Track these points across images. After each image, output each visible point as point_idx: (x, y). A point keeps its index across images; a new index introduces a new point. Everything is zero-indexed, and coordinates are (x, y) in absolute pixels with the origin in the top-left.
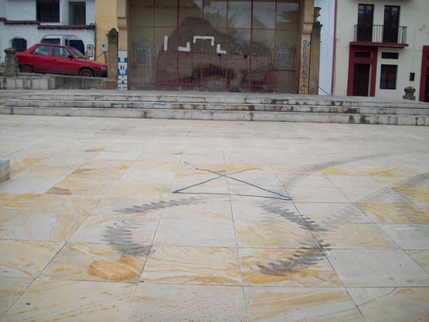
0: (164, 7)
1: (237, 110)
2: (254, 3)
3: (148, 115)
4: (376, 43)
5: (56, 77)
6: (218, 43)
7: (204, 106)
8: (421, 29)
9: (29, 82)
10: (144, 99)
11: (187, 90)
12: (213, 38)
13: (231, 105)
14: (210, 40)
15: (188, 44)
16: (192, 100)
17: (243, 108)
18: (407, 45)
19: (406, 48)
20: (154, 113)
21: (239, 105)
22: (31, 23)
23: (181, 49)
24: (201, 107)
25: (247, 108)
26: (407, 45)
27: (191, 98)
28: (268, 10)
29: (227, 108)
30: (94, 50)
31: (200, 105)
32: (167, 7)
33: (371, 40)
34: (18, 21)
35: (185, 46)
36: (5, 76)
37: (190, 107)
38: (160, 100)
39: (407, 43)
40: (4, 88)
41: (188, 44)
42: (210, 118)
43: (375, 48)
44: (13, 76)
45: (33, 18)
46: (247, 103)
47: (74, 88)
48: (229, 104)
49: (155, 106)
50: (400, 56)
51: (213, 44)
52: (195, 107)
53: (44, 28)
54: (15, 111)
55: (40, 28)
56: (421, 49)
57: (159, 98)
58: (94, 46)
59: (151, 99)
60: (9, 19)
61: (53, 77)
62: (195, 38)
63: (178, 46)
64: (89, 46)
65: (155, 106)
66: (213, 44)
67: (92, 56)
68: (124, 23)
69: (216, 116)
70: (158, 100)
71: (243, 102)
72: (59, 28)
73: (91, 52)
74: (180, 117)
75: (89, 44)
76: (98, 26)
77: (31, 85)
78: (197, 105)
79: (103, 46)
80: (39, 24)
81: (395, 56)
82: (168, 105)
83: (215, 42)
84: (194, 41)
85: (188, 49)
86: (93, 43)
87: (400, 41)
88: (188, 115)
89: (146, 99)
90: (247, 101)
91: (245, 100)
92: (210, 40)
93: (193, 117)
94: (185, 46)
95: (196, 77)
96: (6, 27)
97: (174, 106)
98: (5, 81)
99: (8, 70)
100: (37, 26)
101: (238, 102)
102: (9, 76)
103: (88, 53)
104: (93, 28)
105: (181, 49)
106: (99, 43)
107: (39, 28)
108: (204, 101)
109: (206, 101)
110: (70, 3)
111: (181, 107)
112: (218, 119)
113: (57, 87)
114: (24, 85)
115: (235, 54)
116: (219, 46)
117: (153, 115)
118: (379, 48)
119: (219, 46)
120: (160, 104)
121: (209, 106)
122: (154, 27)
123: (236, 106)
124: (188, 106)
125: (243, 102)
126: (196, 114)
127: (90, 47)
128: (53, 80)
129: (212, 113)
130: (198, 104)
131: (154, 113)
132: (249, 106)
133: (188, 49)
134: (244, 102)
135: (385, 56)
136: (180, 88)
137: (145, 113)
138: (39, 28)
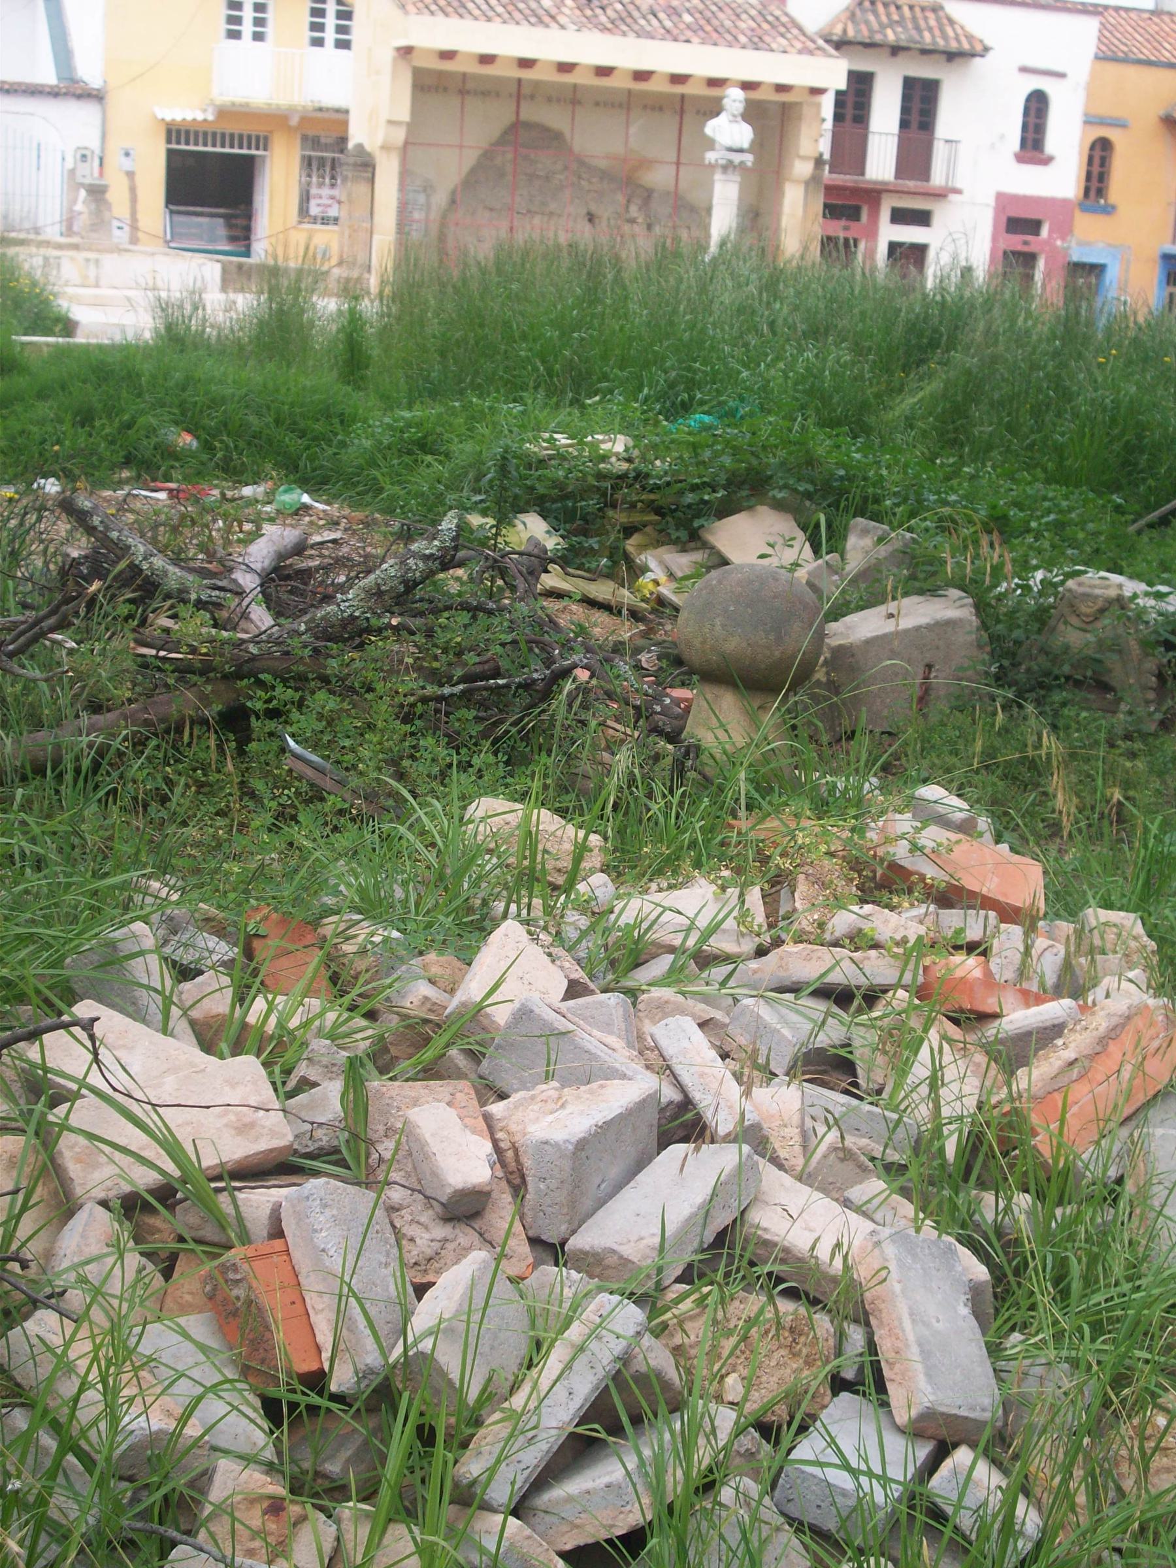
4: (876, 182)
8: (993, 146)
18: (958, 191)
19: (953, 197)
26: (958, 191)
28: (698, 112)
33: (863, 174)
39: (958, 185)
43: (873, 195)
50: (936, 220)
56: (992, 202)
58: (98, 152)
68: (400, 135)
73: (87, 172)
75: (80, 145)
79: (127, 154)
81: (922, 218)
86: (94, 144)
87: (938, 177)
103: (79, 173)
118: (884, 196)
122: (461, 147)
127: (84, 156)
135: (900, 217)
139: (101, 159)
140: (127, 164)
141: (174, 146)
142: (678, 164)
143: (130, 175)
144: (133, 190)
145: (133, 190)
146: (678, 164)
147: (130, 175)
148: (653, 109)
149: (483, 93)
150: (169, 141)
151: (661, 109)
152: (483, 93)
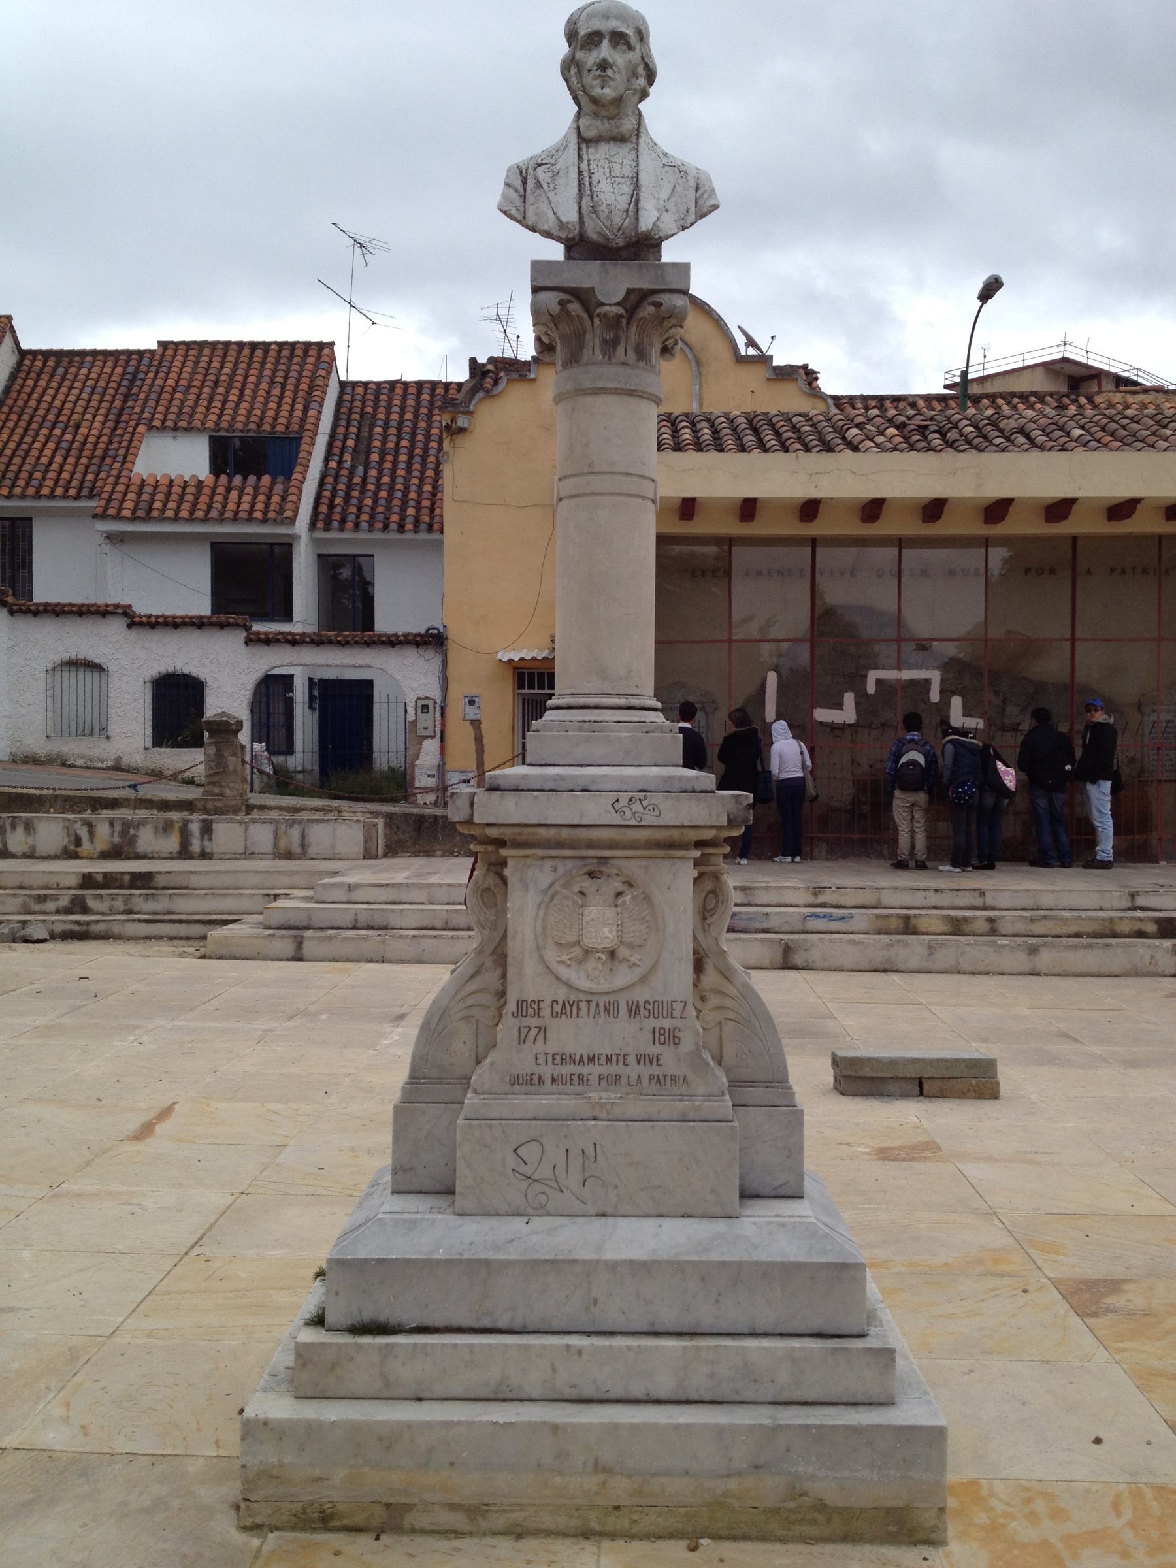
0: (747, 574)
1: (1115, 935)
2: (904, 551)
3: (798, 959)
5: (390, 817)
6: (954, 693)
7: (991, 920)
9: (295, 833)
10: (763, 897)
11: (844, 856)
12: (935, 676)
13: (1090, 918)
14: (927, 682)
15: (849, 698)
16: (945, 899)
17: (1137, 926)
20: (818, 947)
21: (1121, 918)
22: (198, 623)
23: (822, 715)
24: (983, 926)
25: (1151, 928)
27: (932, 893)
28: (1112, 570)
29: (1073, 929)
30: (438, 715)
31: (975, 918)
32: (759, 573)
34: (174, 617)
35: (839, 706)
36: (206, 811)
37: (941, 926)
38: (821, 899)
40: (204, 855)
41: (849, 698)
42: (1026, 968)
44: (236, 811)
45: (202, 606)
46: (1142, 909)
47: (451, 854)
48: (1084, 914)
49: (812, 924)
51: (935, 696)
52: (957, 927)
53: (268, 641)
54: (308, 948)
55: (253, 640)
57: (815, 895)
58: (439, 701)
59: (790, 897)
60: (143, 607)
61: (376, 814)
62: (873, 676)
63: (813, 707)
64: (420, 703)
65: (812, 924)
66: (935, 696)
67: (432, 737)
69: (1046, 958)
70: (811, 899)
71: (1126, 903)
72: (293, 641)
73: (429, 724)
74: (914, 963)
76: (452, 634)
77: (303, 846)
78: (966, 920)
79: (472, 702)
80: (248, 629)
82: (861, 919)
83: (942, 692)
84: (871, 689)
85: (847, 714)
86: (436, 694)
88: (945, 957)
89: (773, 898)
90: (1141, 901)
91: (1133, 896)
92: (927, 682)
93: (965, 966)
94: (839, 706)
95: (866, 809)
96: (134, 635)
97: (881, 924)
98: (207, 830)
99: (216, 790)
100: (245, 634)
101: (1106, 905)
102: (219, 812)
103: (420, 726)
104: (432, 640)
105: (822, 715)
106: (456, 694)
107: (248, 642)
108: (979, 902)
109: (989, 900)
110: (319, 556)
111: (908, 927)
112: (1057, 970)
113: (393, 850)
114: (275, 845)
115: (1004, 729)
116: (956, 702)
117: (815, 956)
119: (956, 702)
120: (830, 917)
121: (1010, 921)
123: (1111, 920)
124: (931, 921)
125: (1126, 903)
126: (973, 949)
127: (425, 707)
128: (380, 822)
129: (1033, 950)
130: (967, 913)
131: (818, 947)
132: (1158, 921)
133: (847, 714)
134: (1129, 904)
136: (824, 847)
137: (787, 949)
138: (248, 642)
139: (443, 709)
140: (472, 713)
141: (526, 691)
142: (1073, 640)
143: (476, 724)
144: (479, 739)
145: (479, 739)
146: (1073, 640)
147: (476, 724)
148: (1040, 572)
149: (780, 573)
150: (521, 687)
151: (1052, 571)
152: (780, 573)
